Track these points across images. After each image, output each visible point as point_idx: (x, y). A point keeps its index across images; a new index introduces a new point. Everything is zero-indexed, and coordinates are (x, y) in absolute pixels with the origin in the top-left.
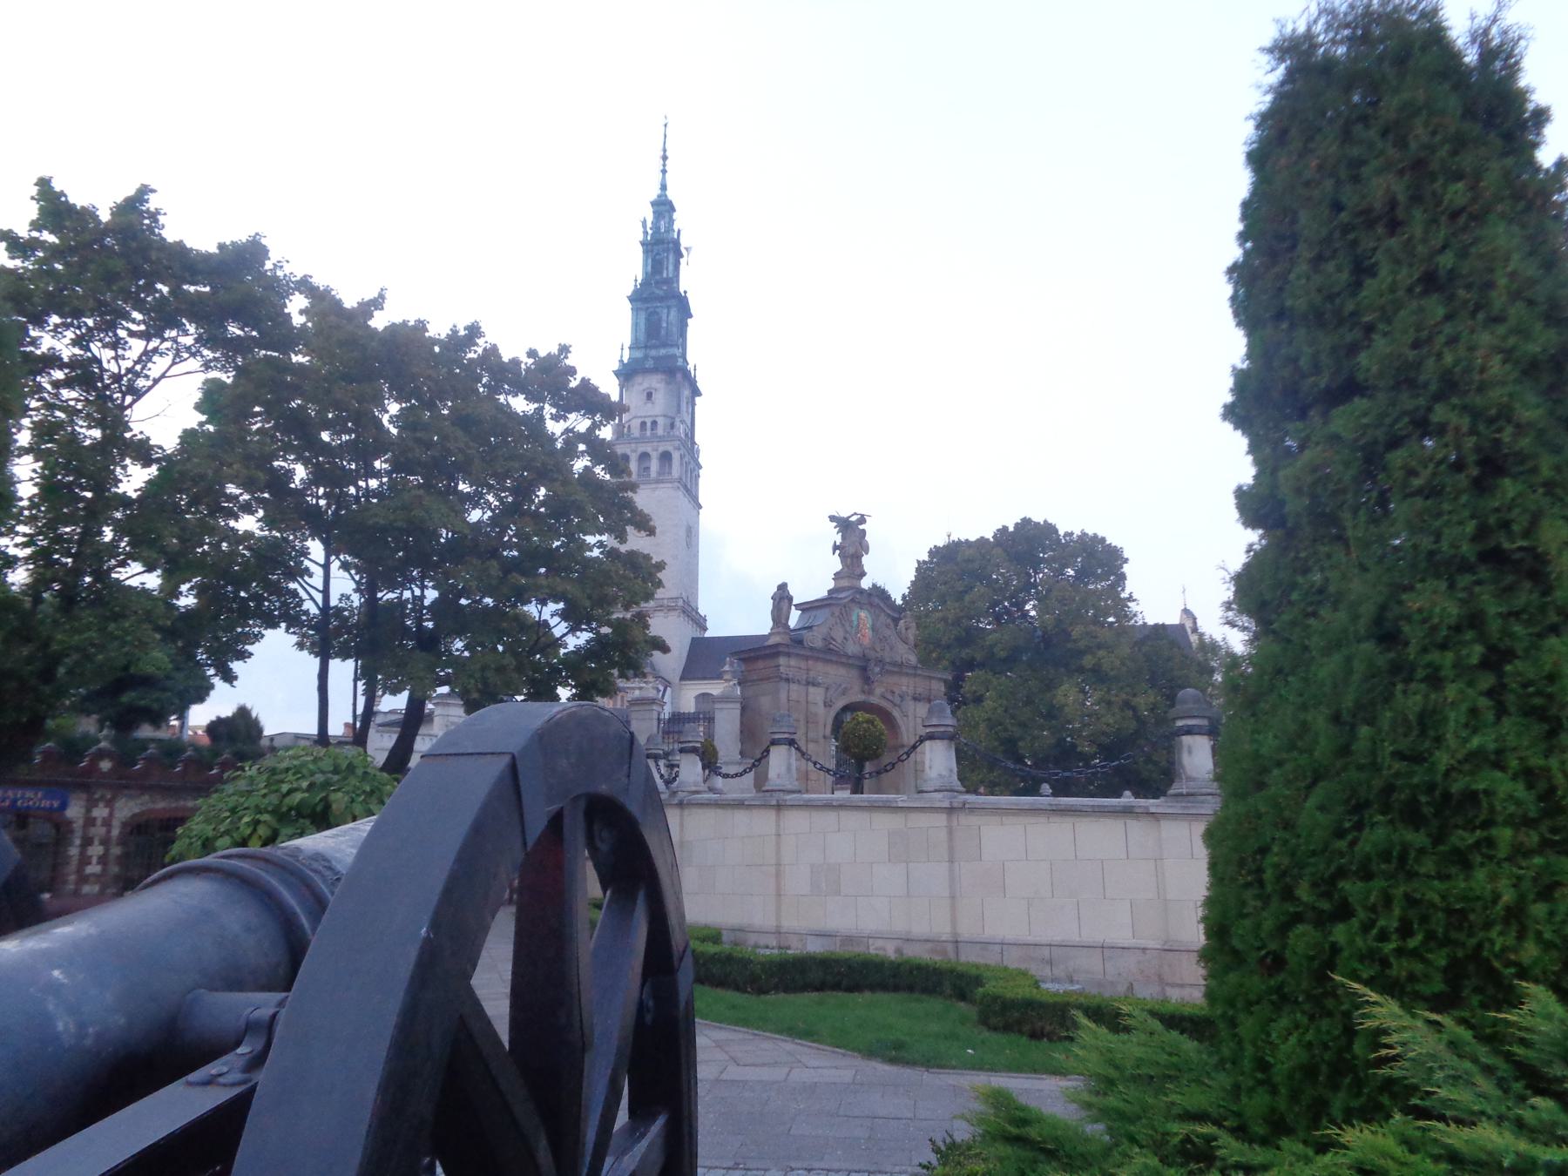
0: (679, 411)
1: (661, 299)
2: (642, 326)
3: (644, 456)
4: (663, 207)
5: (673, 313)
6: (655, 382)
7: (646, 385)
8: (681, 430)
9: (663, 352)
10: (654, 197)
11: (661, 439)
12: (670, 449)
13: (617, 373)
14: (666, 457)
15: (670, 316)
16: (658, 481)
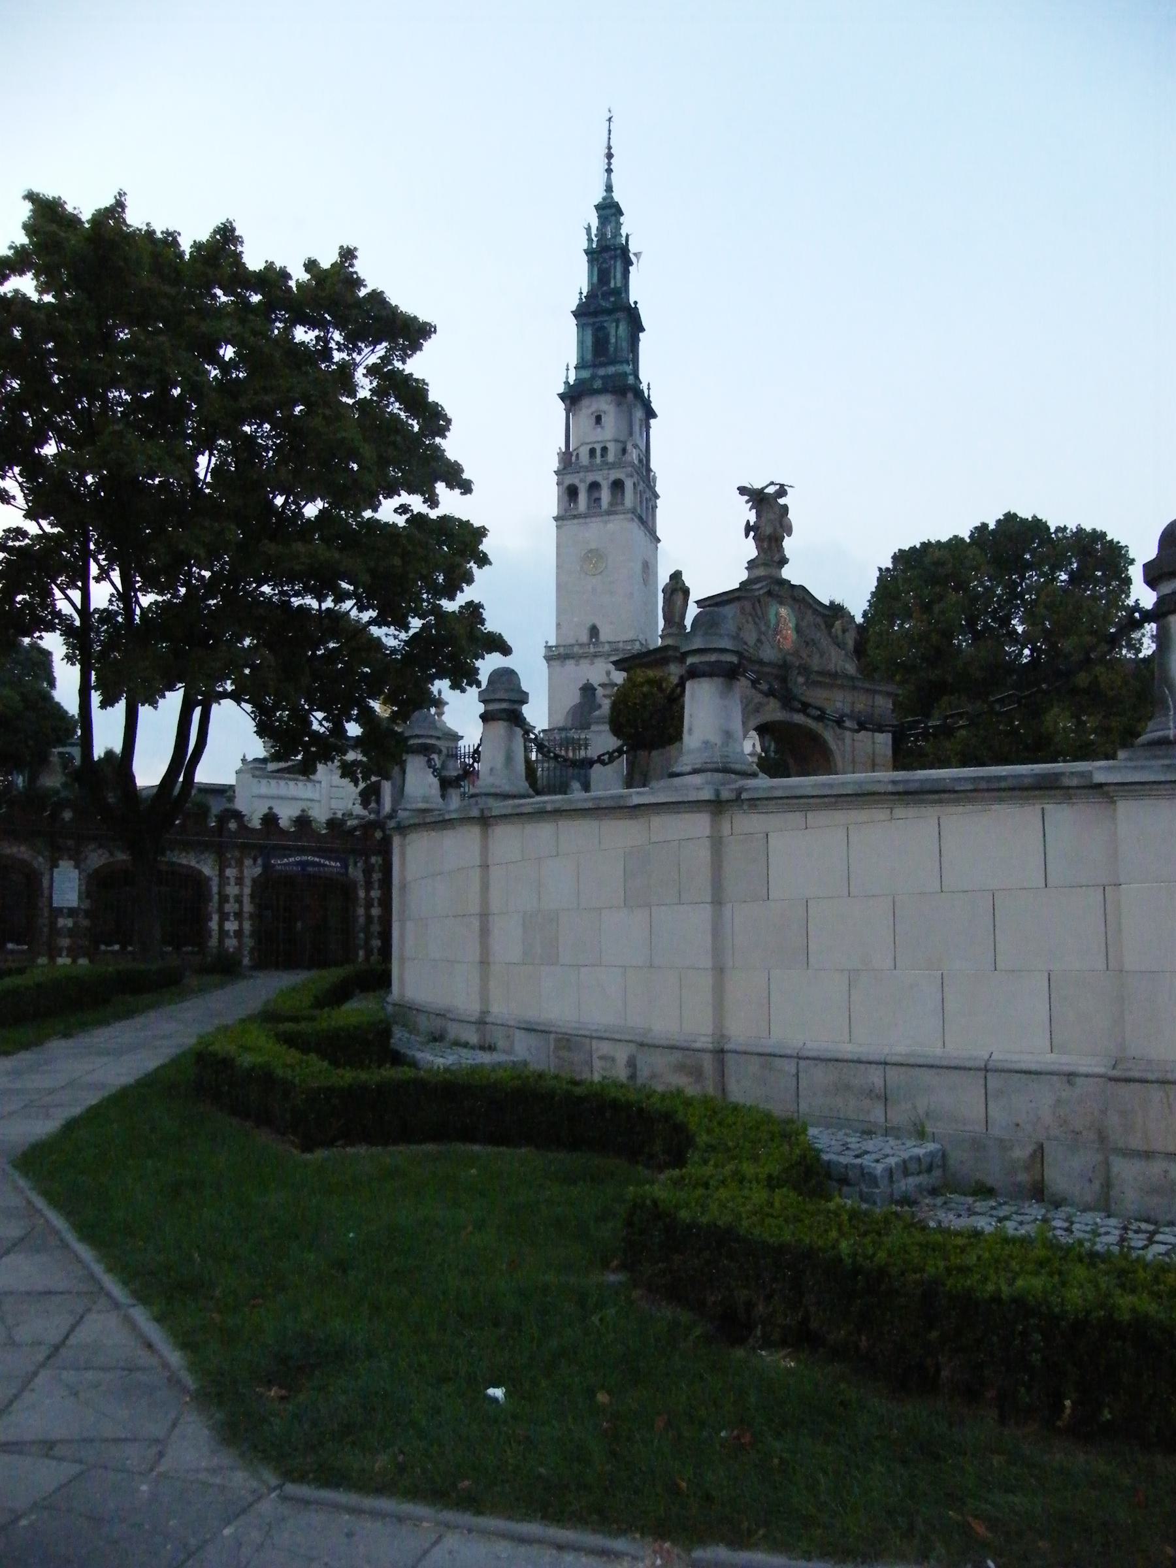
0: (631, 434)
1: (609, 312)
3: (594, 486)
4: (609, 211)
5: (622, 327)
6: (604, 404)
7: (593, 409)
8: (634, 455)
9: (611, 370)
11: (612, 466)
13: (562, 397)
14: (618, 485)
15: (618, 332)
16: (609, 513)
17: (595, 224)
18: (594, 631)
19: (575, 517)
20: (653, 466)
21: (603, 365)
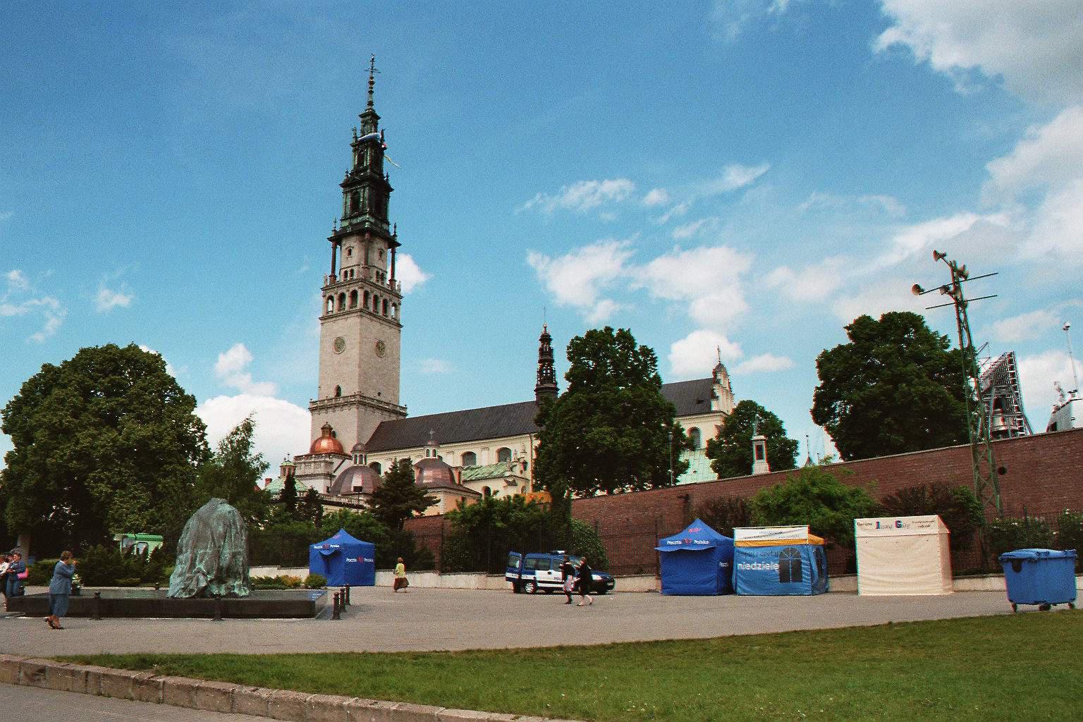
1: (359, 183)
2: (349, 203)
3: (342, 297)
5: (367, 191)
6: (353, 243)
9: (359, 219)
10: (363, 112)
11: (352, 282)
12: (356, 288)
13: (330, 239)
14: (354, 294)
16: (349, 313)
17: (359, 126)
18: (338, 389)
19: (331, 317)
20: (396, 278)
21: (356, 217)
